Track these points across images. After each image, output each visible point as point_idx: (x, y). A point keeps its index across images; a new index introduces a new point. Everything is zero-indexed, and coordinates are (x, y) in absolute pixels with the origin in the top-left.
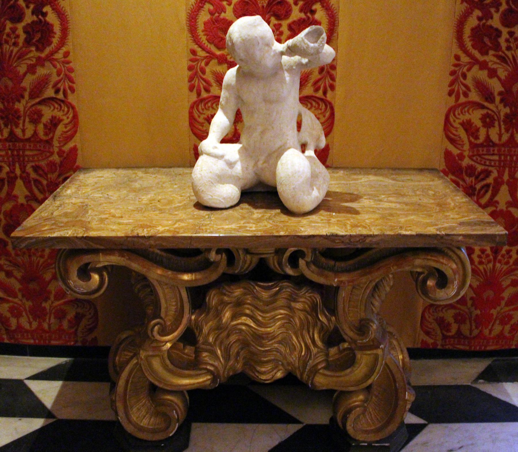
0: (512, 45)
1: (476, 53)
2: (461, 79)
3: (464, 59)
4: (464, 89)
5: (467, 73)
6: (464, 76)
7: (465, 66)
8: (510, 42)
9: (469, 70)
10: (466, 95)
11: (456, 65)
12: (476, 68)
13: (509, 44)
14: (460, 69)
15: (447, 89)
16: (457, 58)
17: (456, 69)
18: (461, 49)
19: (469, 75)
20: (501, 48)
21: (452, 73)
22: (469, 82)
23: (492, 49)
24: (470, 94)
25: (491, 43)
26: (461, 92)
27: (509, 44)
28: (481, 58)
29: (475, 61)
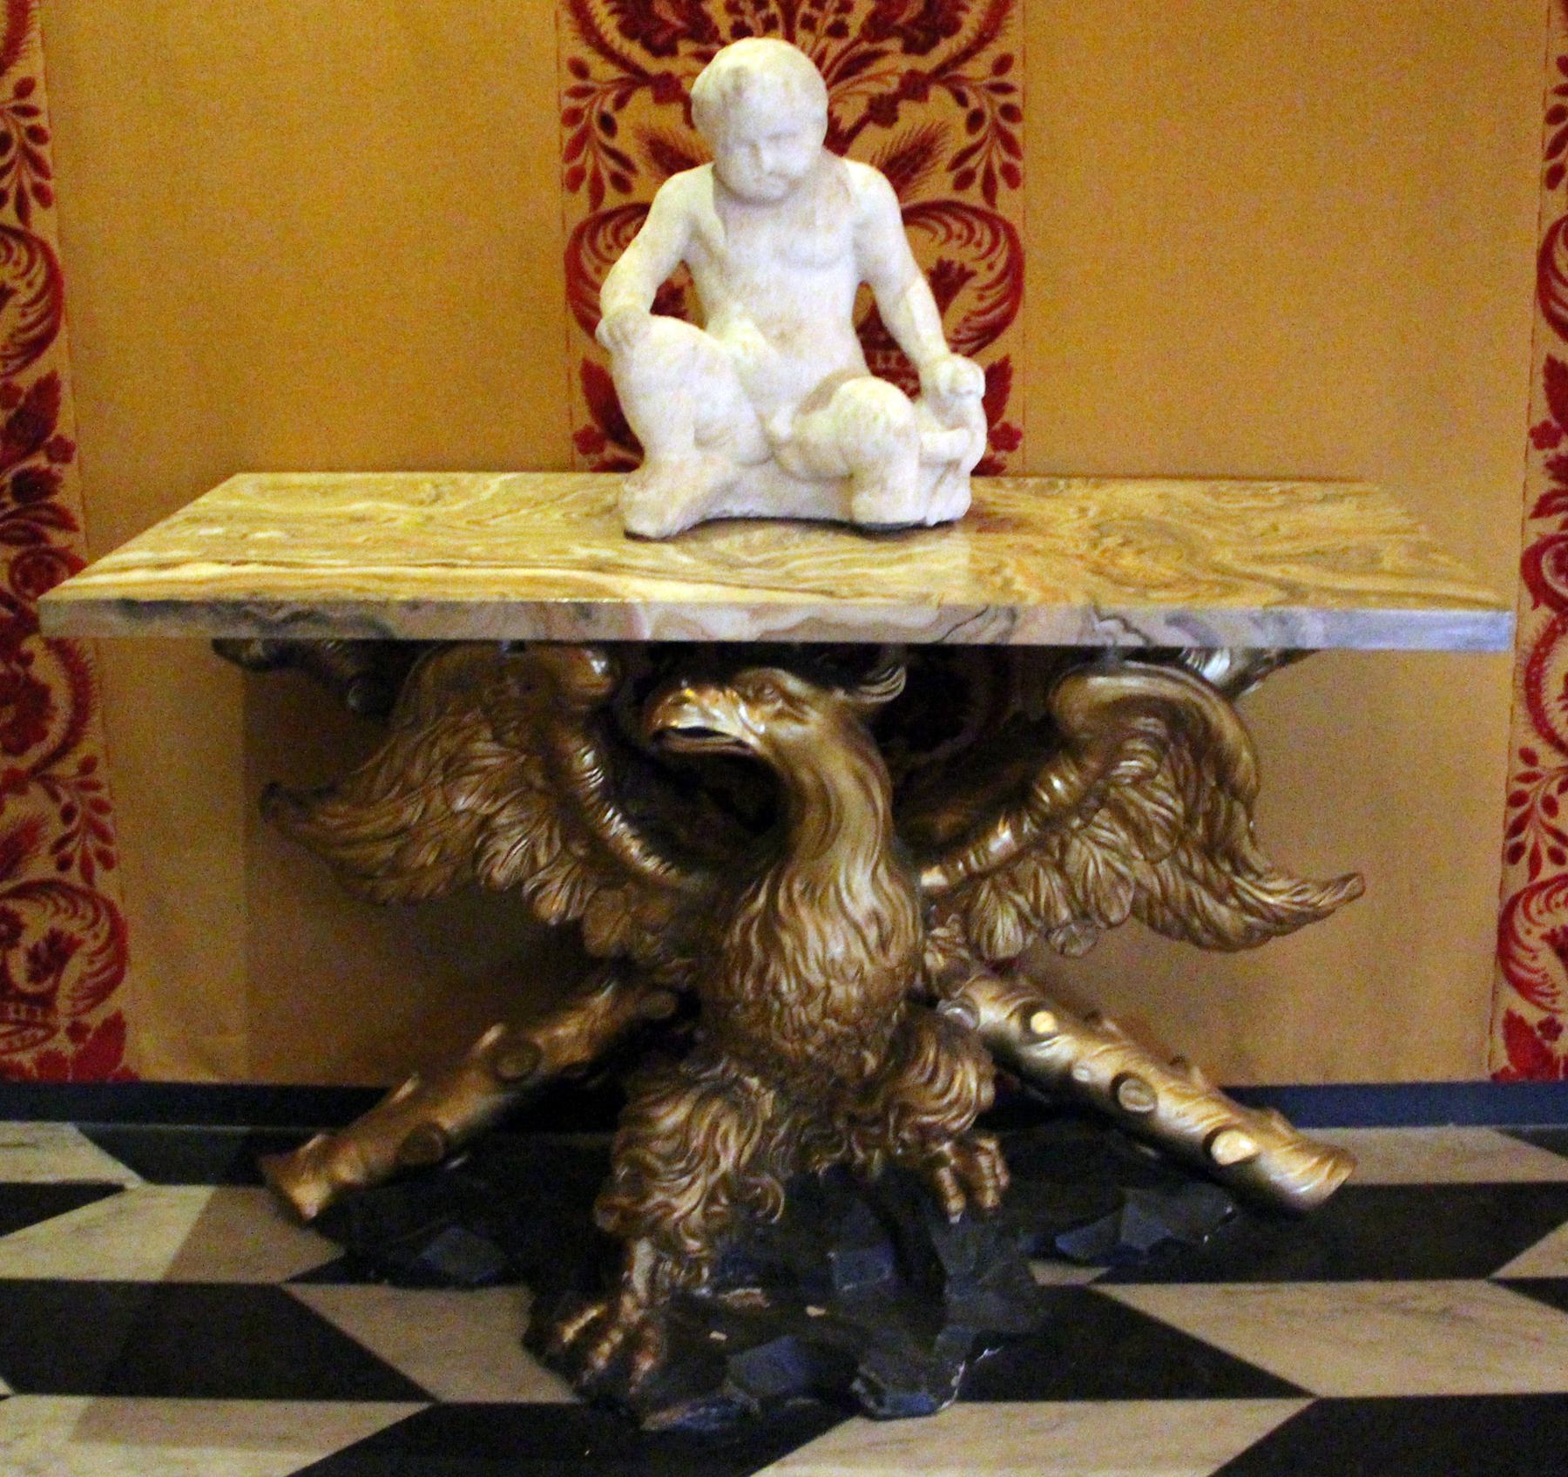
0: (748, 21)
1: (635, 51)
2: (600, 134)
3: (604, 71)
4: (612, 164)
5: (615, 116)
6: (608, 125)
7: (607, 92)
8: (742, 12)
9: (620, 103)
10: (622, 184)
11: (578, 93)
12: (642, 98)
13: (738, 18)
14: (592, 104)
15: (558, 168)
16: (580, 69)
17: (582, 103)
18: (589, 42)
19: (623, 120)
20: (717, 31)
21: (572, 117)
22: (626, 142)
23: (683, 37)
24: (635, 182)
25: (683, 18)
26: (605, 175)
27: (738, 18)
28: (654, 66)
29: (636, 78)
